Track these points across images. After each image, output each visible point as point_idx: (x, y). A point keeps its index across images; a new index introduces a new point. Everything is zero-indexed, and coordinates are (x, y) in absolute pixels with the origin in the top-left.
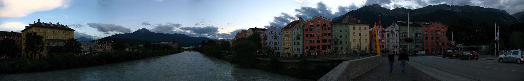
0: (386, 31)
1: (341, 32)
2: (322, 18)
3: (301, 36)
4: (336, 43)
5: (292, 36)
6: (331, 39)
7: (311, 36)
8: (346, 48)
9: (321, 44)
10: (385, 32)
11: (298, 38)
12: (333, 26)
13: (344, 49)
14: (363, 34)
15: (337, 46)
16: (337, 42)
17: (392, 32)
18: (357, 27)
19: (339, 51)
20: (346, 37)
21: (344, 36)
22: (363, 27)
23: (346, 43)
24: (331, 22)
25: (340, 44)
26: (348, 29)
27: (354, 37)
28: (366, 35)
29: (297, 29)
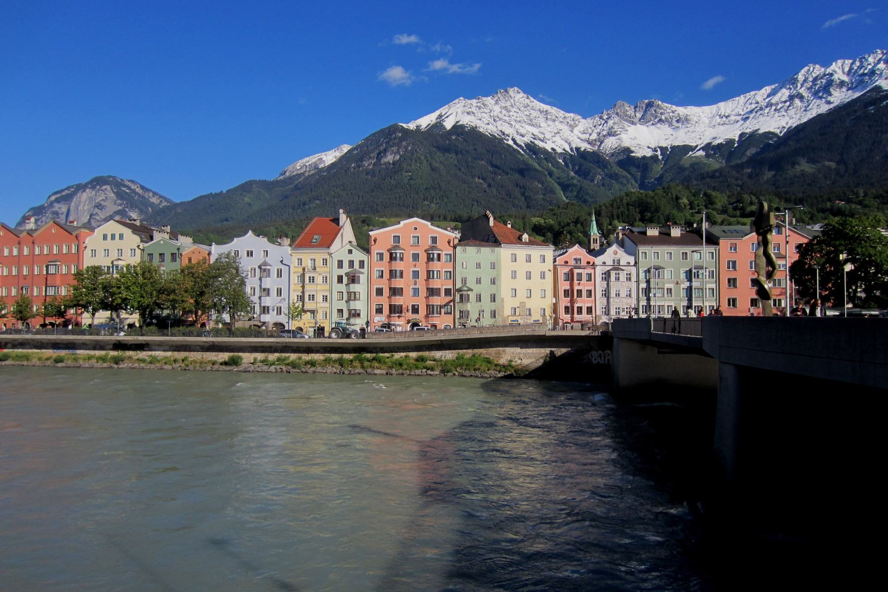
0: (596, 263)
2: (427, 225)
3: (363, 273)
8: (494, 314)
10: (594, 266)
11: (353, 279)
13: (487, 314)
14: (536, 276)
20: (493, 282)
21: (486, 281)
23: (493, 298)
28: (544, 278)
29: (350, 252)
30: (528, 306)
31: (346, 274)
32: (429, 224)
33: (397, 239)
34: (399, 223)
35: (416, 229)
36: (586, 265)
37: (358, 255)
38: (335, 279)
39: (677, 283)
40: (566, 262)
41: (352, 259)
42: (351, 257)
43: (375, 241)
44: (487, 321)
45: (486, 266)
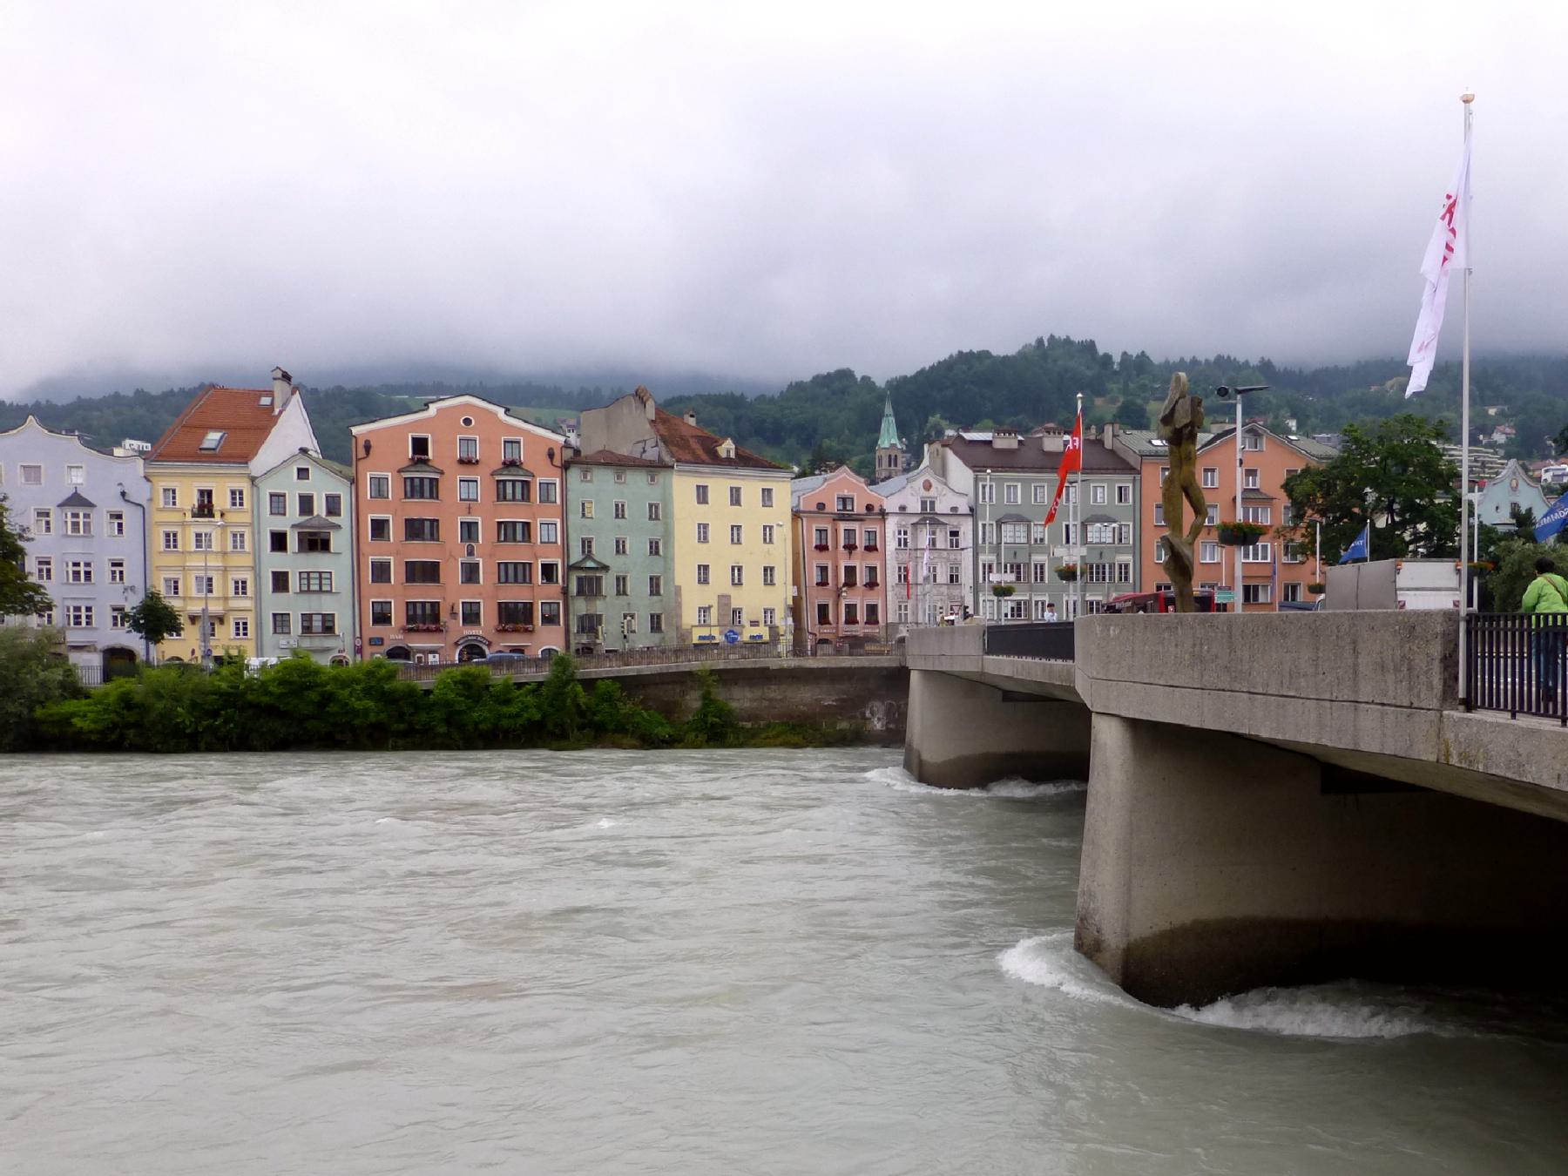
1: (623, 517)
2: (495, 415)
4: (590, 588)
5: (255, 525)
7: (415, 529)
8: (656, 623)
9: (488, 595)
10: (883, 514)
12: (574, 474)
13: (641, 625)
14: (752, 535)
15: (599, 607)
16: (599, 579)
17: (929, 516)
18: (719, 486)
19: (609, 636)
20: (654, 549)
21: (637, 546)
22: (752, 485)
23: (655, 586)
24: (557, 452)
25: (618, 593)
26: (667, 498)
29: (303, 473)
30: (733, 606)
31: (294, 526)
32: (500, 412)
33: (420, 445)
36: (865, 511)
37: (322, 484)
38: (267, 542)
40: (821, 506)
41: (306, 492)
42: (305, 487)
43: (368, 448)
44: (643, 638)
45: (637, 511)
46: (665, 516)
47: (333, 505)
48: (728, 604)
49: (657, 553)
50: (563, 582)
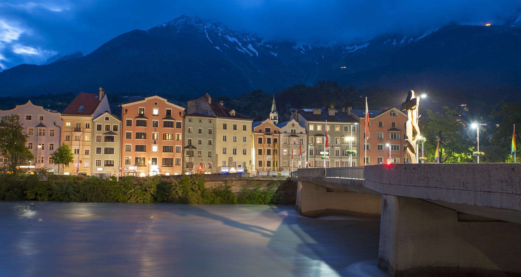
1: (201, 133)
6: (181, 146)
10: (279, 133)
21: (205, 141)
27: (224, 145)
34: (144, 99)
35: (156, 104)
39: (333, 147)
43: (126, 110)
46: (213, 133)
47: (115, 128)
48: (232, 160)
49: (211, 144)
50: (182, 151)
